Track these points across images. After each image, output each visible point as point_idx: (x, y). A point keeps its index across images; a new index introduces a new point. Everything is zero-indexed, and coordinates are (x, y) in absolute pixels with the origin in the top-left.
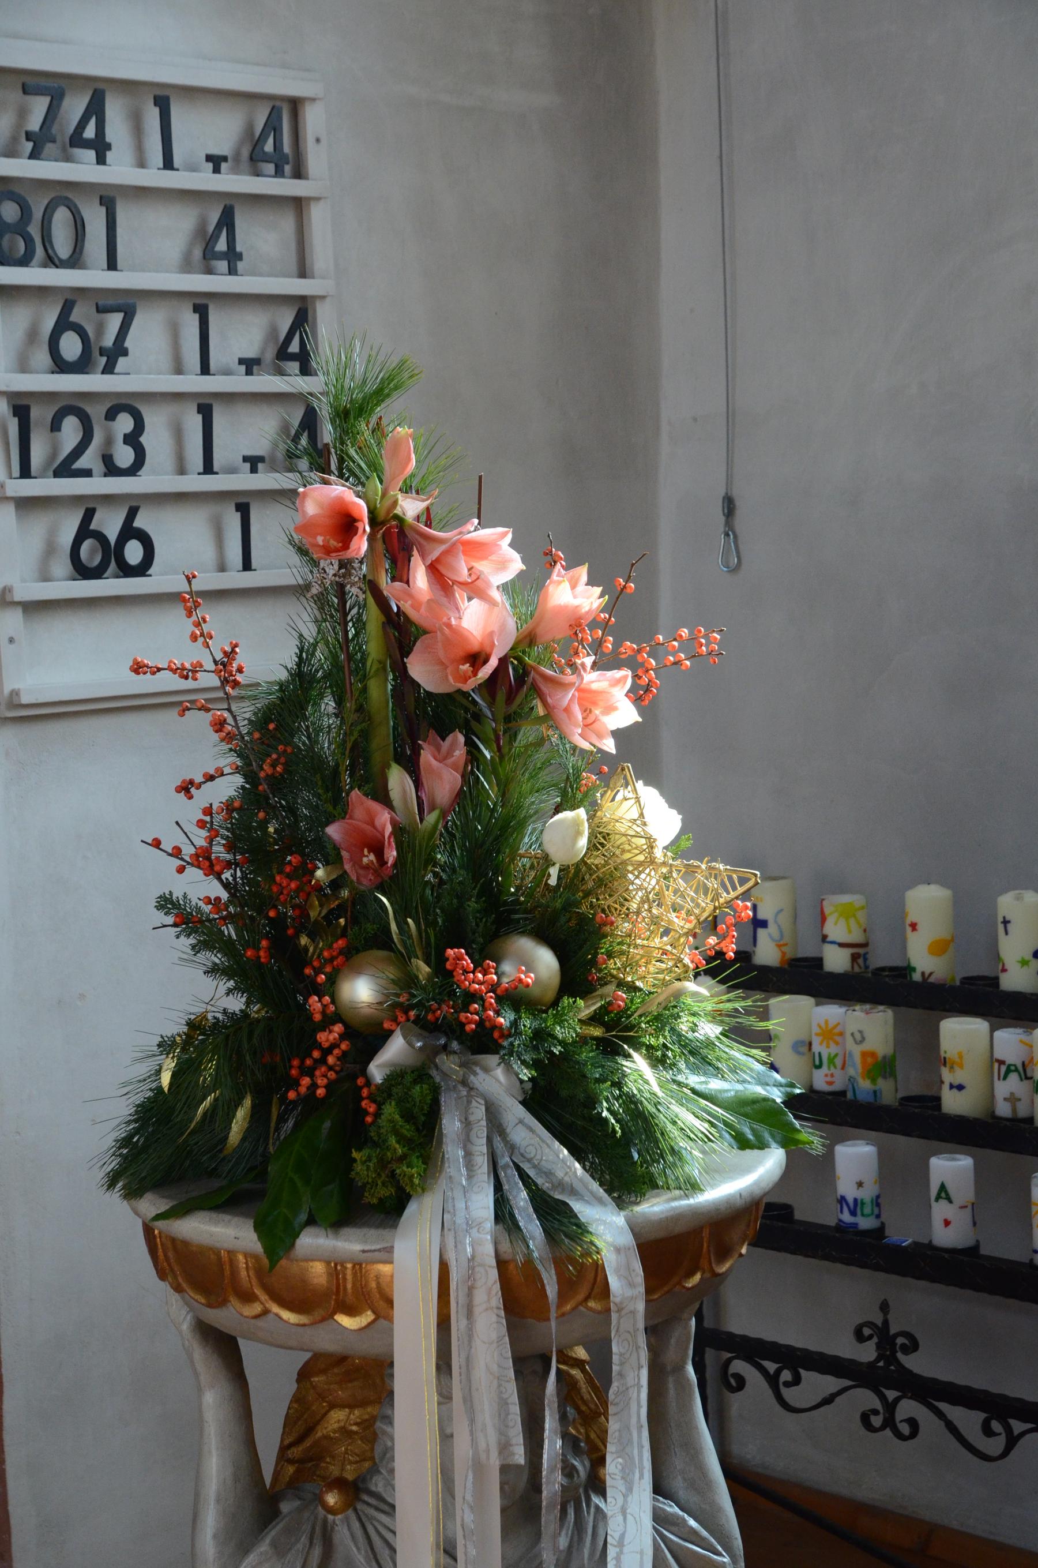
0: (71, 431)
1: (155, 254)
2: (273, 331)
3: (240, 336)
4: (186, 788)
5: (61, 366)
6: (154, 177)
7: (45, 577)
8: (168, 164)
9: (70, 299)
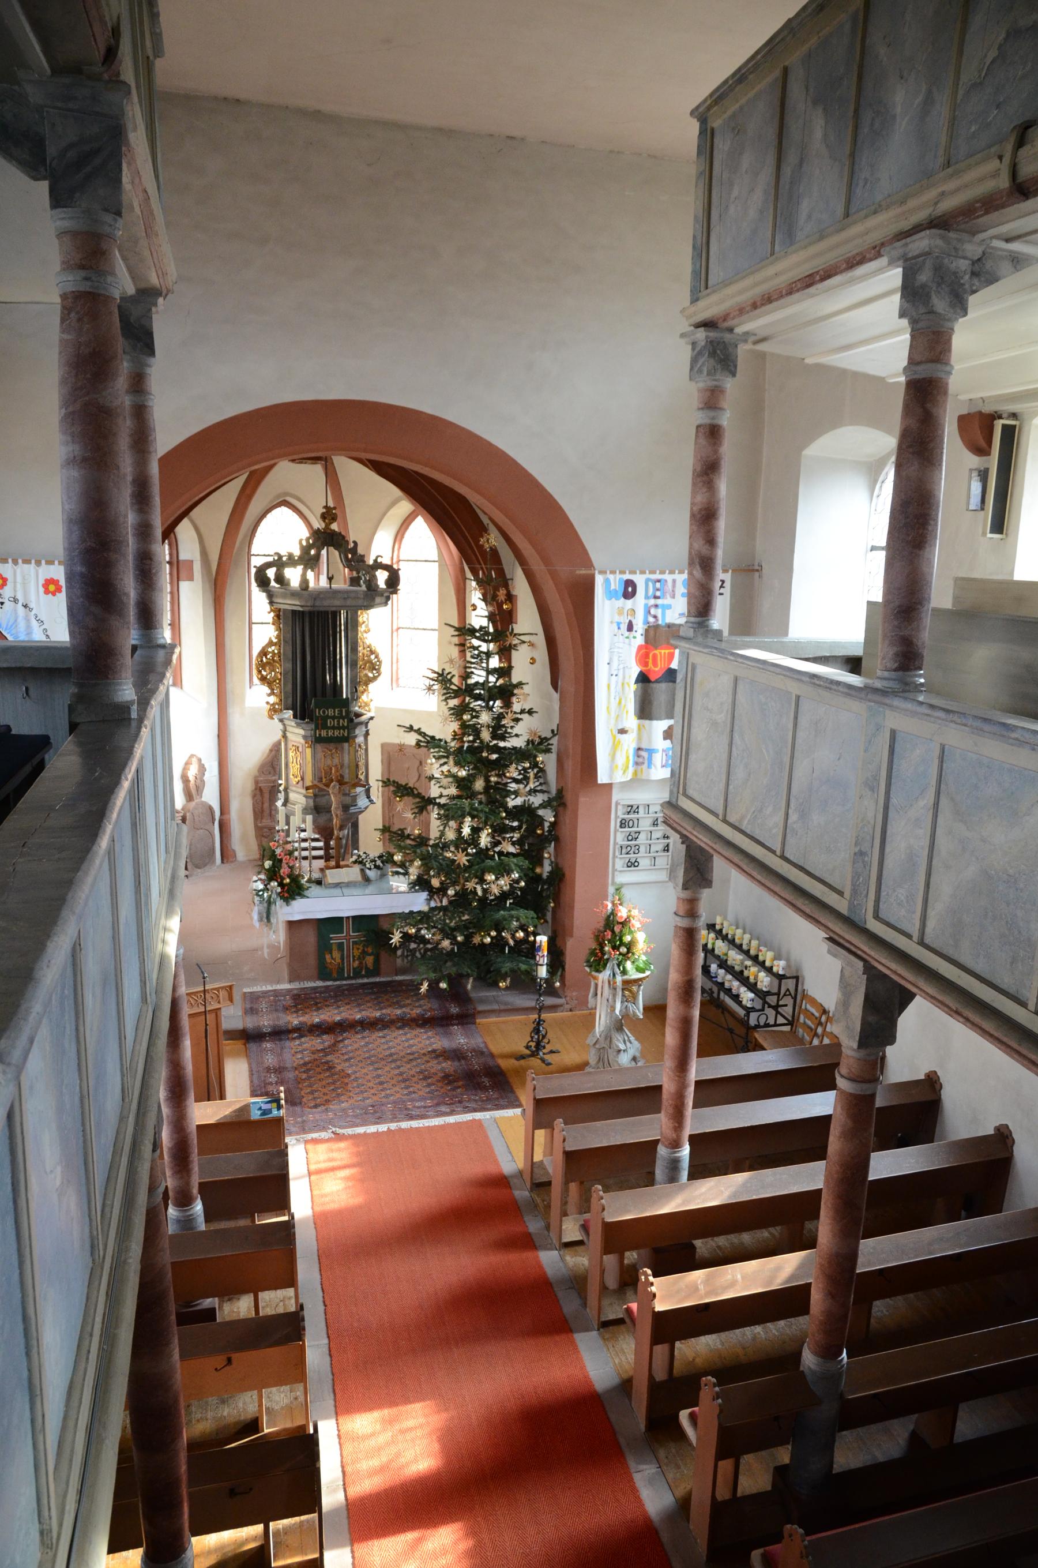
1: (645, 825)
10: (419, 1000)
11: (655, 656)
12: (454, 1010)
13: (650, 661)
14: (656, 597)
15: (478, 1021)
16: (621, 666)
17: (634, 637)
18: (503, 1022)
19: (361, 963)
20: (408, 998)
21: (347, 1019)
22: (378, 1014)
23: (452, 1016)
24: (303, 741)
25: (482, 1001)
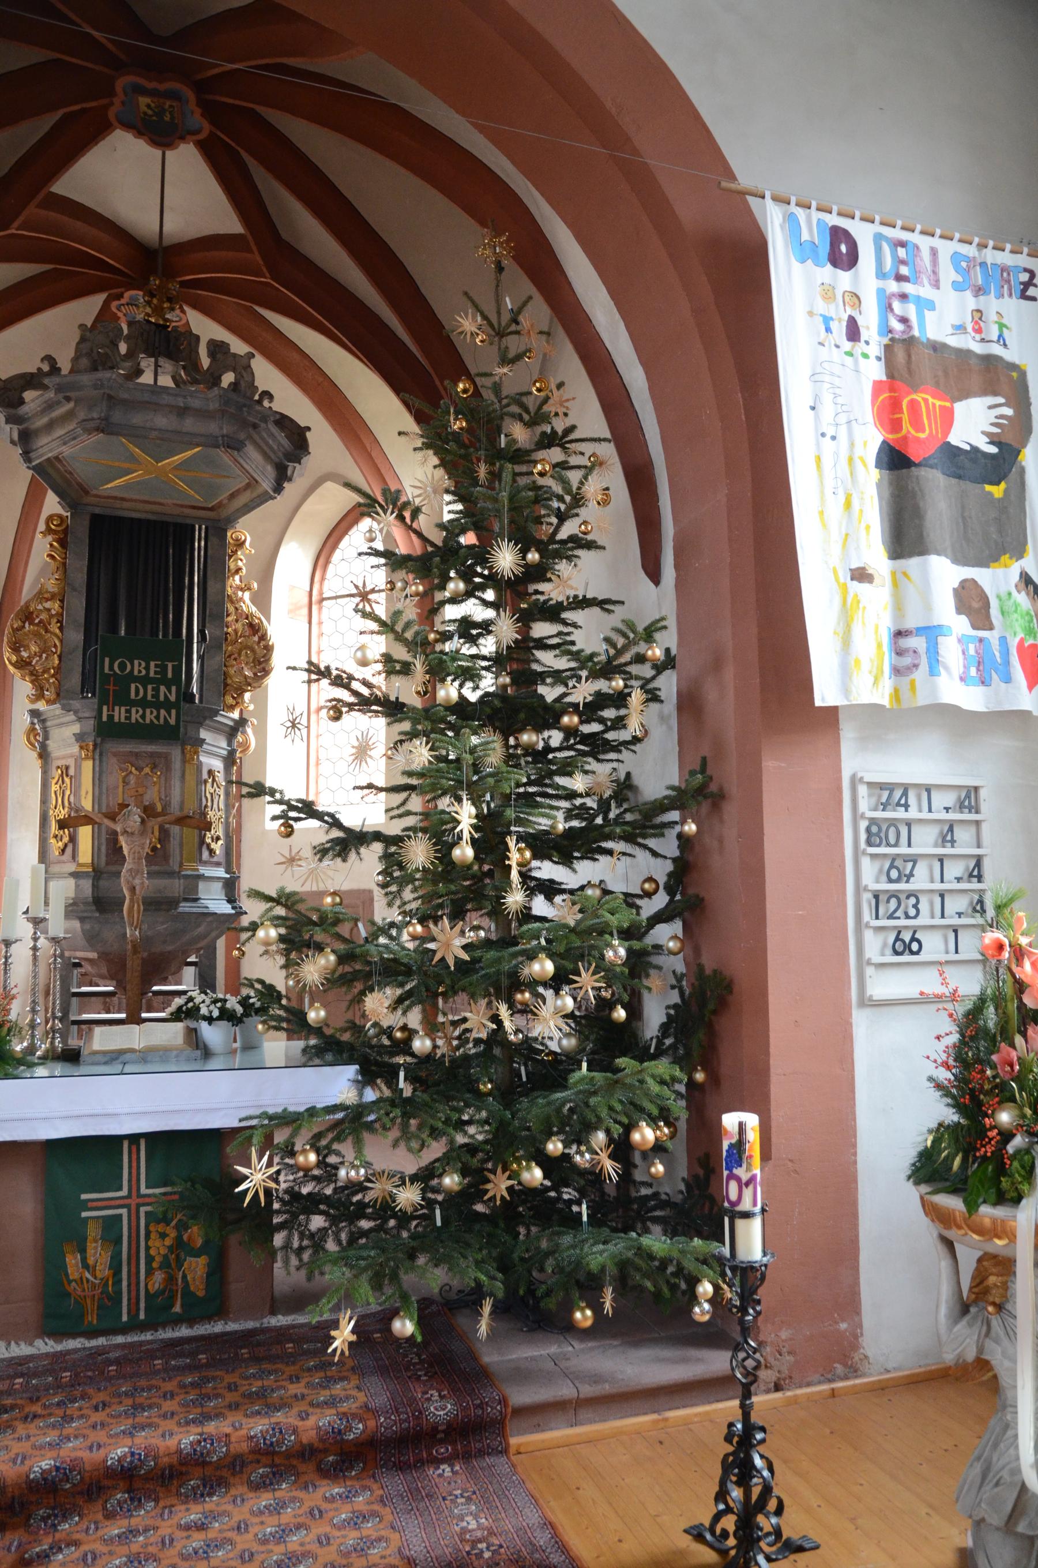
0: (893, 903)
1: (925, 841)
2: (967, 868)
3: (955, 869)
4: (938, 1038)
5: (890, 881)
6: (925, 815)
7: (883, 954)
8: (930, 811)
9: (894, 858)
10: (328, 1382)
11: (914, 405)
12: (440, 1408)
13: (905, 417)
14: (900, 278)
15: (514, 1441)
16: (843, 419)
17: (866, 356)
18: (590, 1441)
19: (170, 1279)
20: (294, 1379)
21: (75, 1465)
22: (186, 1439)
23: (435, 1429)
24: (75, 749)
25: (523, 1375)
